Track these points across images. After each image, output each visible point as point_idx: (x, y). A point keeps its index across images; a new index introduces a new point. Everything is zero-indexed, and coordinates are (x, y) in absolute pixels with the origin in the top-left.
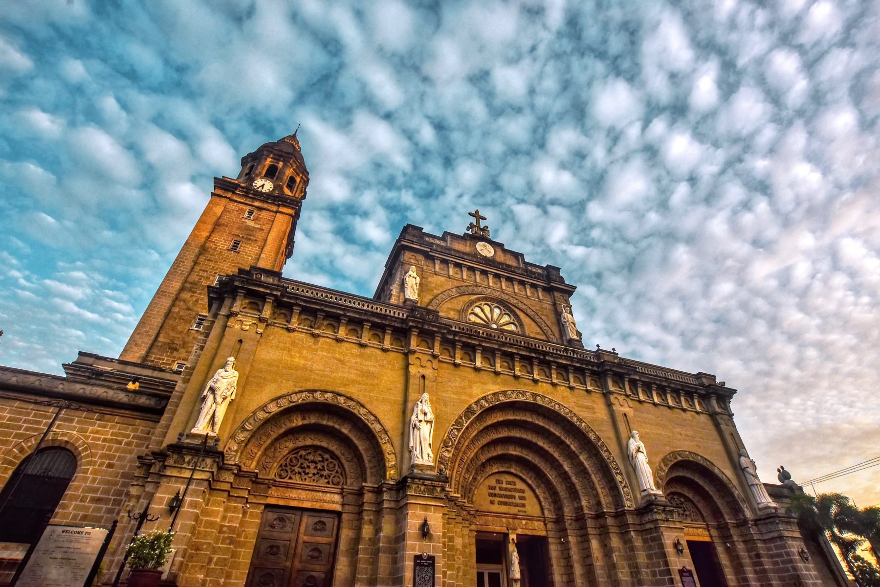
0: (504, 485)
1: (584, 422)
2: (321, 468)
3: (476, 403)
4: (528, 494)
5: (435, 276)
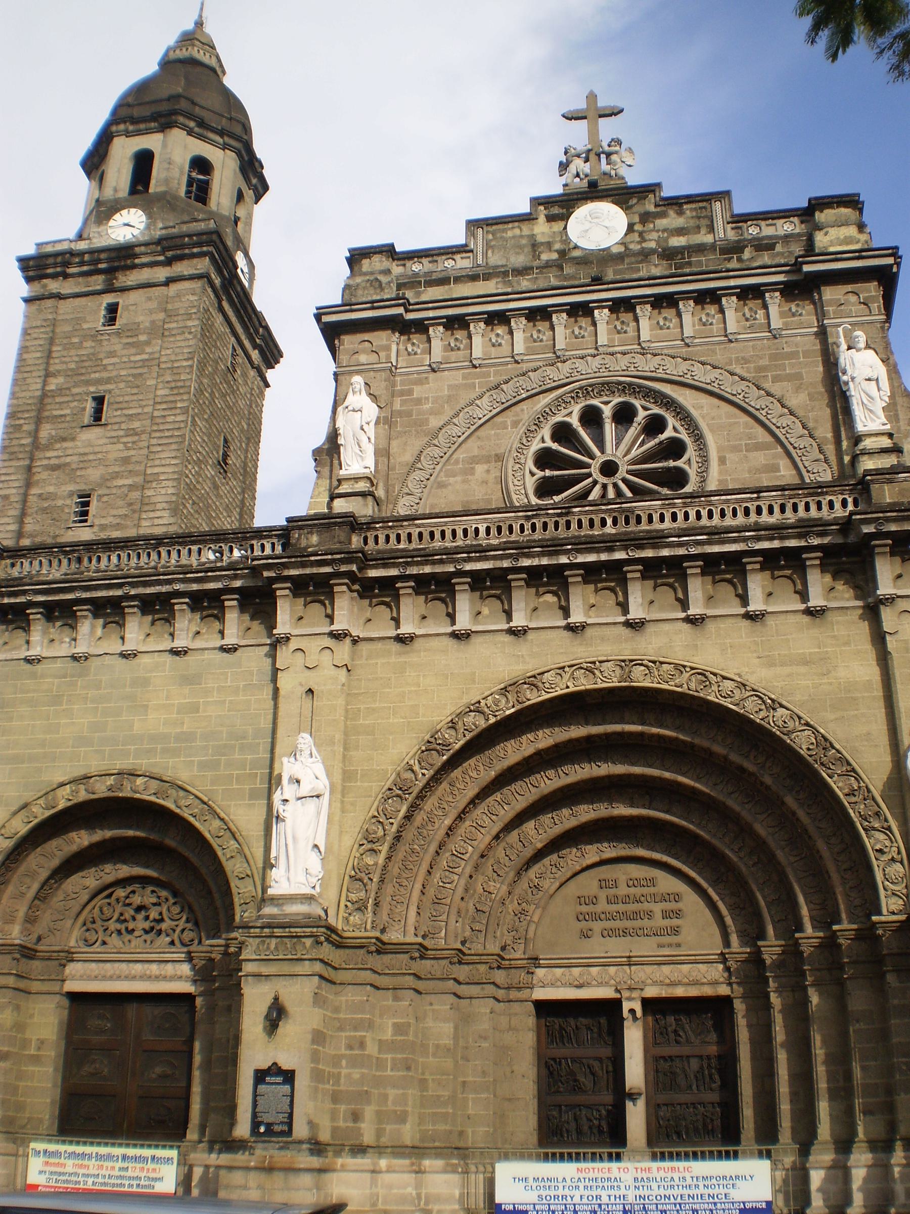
0: (623, 890)
1: (782, 706)
2: (158, 917)
3: (453, 725)
4: (691, 900)
5: (432, 376)
